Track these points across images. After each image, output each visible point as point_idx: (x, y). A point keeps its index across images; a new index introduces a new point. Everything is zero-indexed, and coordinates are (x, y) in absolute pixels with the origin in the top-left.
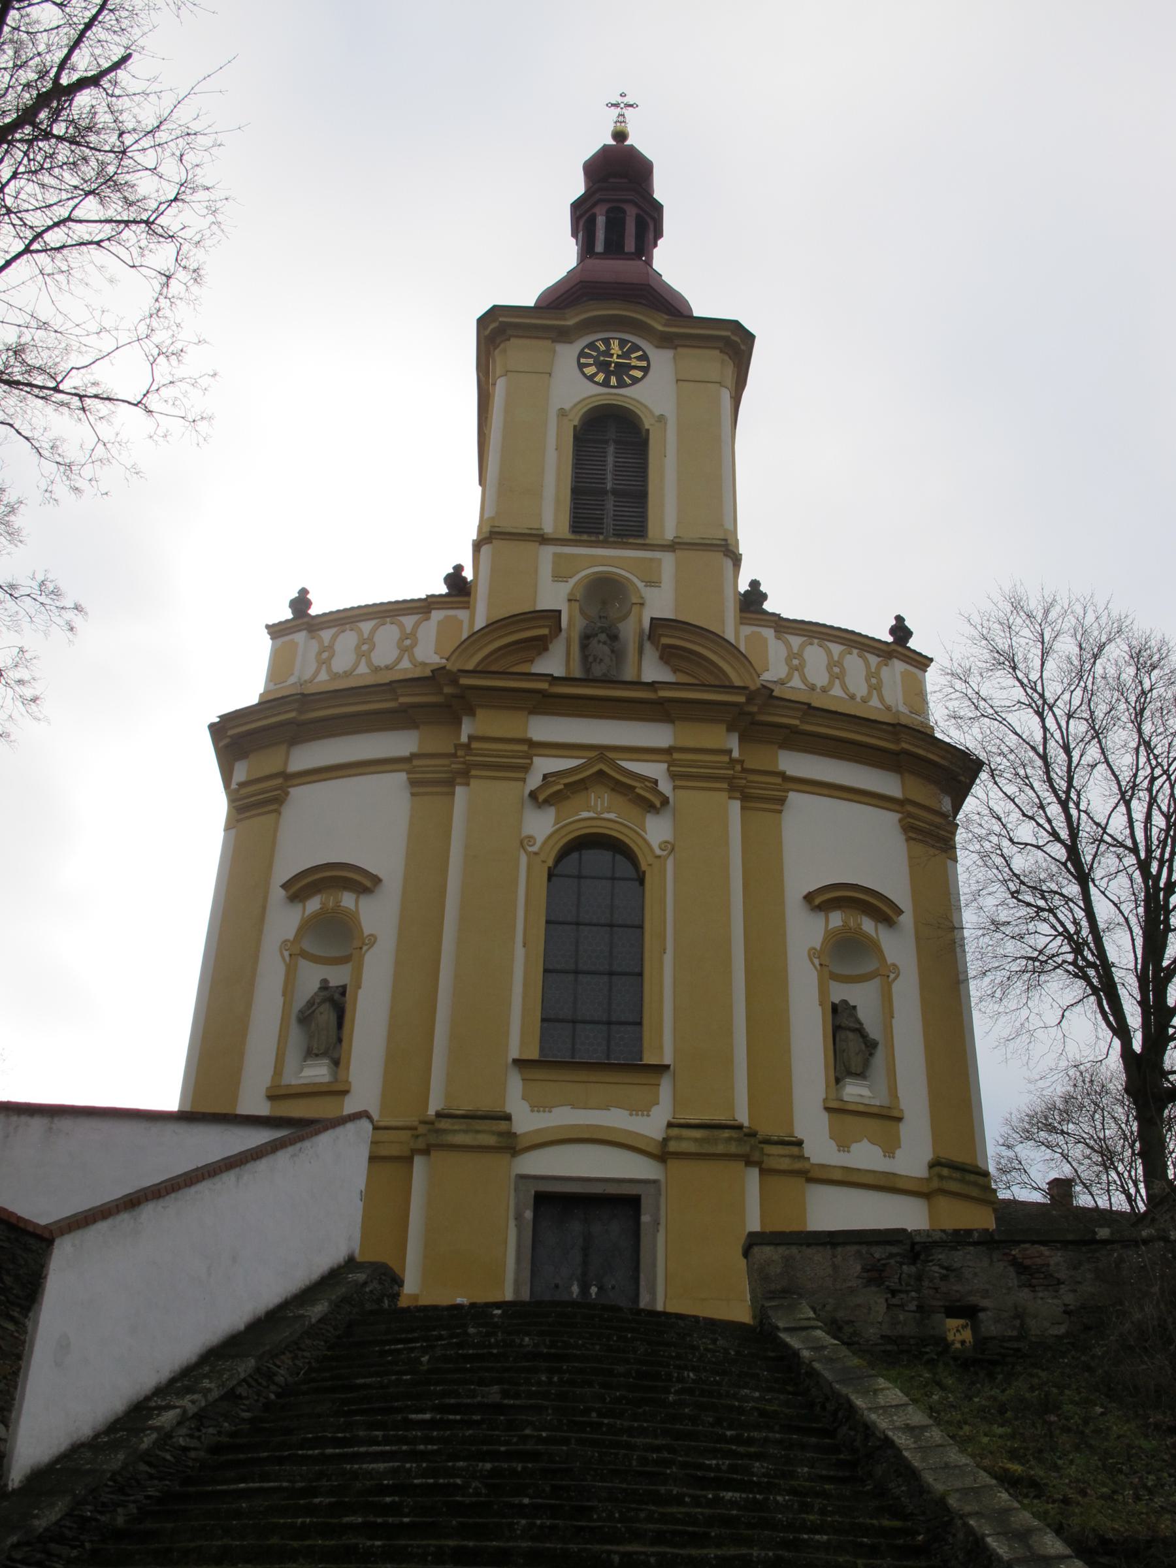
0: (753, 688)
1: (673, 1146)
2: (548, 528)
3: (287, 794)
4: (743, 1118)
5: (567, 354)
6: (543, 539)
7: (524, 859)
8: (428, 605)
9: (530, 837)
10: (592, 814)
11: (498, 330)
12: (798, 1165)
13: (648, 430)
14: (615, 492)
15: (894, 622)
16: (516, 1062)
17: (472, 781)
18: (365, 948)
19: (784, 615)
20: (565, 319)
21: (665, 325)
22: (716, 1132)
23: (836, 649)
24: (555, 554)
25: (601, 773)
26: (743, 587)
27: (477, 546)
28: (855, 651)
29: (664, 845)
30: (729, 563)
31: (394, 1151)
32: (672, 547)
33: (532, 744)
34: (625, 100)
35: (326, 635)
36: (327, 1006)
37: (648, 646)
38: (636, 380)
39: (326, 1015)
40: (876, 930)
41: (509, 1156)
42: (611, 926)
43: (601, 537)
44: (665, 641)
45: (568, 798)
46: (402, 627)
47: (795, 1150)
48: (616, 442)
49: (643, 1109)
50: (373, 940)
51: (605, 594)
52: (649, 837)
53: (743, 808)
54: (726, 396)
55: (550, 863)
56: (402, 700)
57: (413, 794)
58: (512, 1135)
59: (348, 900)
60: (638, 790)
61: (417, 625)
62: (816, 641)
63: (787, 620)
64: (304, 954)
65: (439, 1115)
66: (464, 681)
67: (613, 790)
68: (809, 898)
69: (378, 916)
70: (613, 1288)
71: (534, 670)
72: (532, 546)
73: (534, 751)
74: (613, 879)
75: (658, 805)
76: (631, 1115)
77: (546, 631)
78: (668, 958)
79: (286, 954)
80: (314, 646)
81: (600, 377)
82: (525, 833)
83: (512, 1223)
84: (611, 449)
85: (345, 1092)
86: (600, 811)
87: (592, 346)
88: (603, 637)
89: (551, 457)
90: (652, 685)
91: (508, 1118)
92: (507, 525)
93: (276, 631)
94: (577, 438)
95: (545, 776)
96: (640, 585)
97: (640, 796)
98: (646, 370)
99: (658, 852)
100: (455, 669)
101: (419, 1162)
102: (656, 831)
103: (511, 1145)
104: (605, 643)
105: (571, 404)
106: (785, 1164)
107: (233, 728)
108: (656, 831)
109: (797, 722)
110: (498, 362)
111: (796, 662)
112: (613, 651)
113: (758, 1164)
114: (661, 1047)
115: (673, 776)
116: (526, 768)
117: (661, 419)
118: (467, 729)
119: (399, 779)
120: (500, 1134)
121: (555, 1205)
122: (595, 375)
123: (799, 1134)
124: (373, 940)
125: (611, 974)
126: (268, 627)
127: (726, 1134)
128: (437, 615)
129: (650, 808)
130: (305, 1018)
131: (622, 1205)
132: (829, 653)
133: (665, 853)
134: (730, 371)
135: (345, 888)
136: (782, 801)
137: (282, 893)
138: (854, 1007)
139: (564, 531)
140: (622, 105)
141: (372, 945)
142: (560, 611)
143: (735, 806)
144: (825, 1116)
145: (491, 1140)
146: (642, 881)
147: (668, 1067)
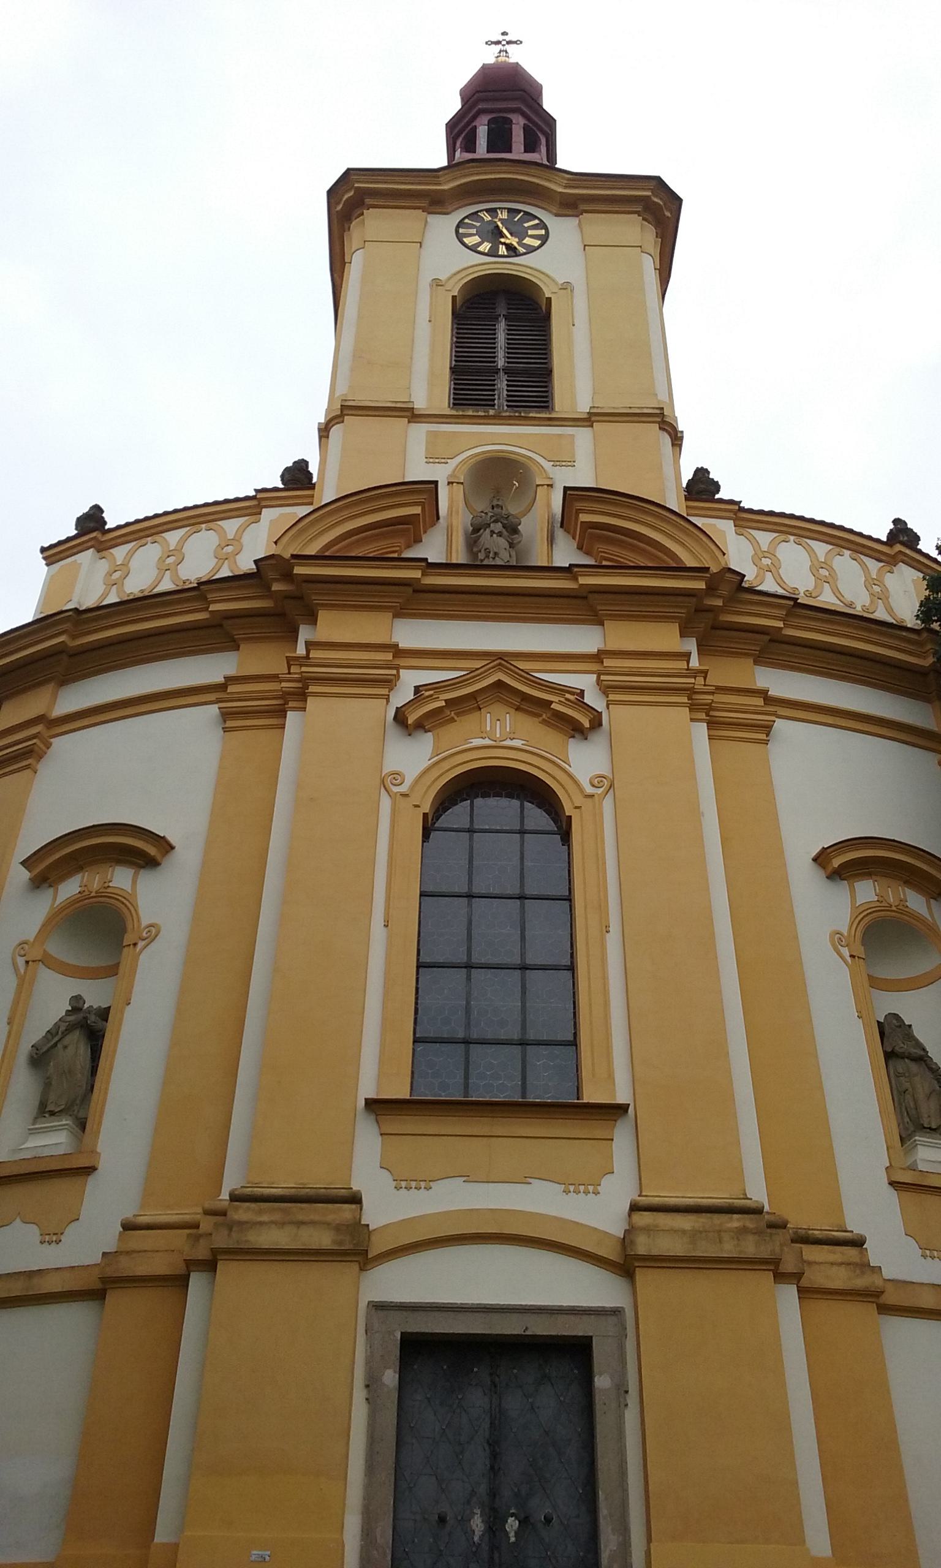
0: (714, 569)
1: (643, 1246)
2: (420, 403)
3: (48, 746)
4: (758, 1193)
5: (442, 226)
6: (412, 415)
7: (386, 803)
8: (254, 505)
10: (487, 742)
11: (356, 198)
12: (860, 1283)
13: (549, 300)
14: (507, 371)
15: (892, 526)
16: (374, 1105)
17: (309, 699)
18: (141, 944)
19: (745, 505)
20: (439, 184)
21: (566, 187)
22: (718, 1219)
23: (821, 549)
25: (499, 684)
26: (687, 475)
27: (324, 432)
28: (847, 553)
29: (597, 780)
30: (667, 440)
31: (159, 1266)
32: (589, 420)
33: (398, 652)
34: (508, 38)
35: (119, 553)
36: (76, 1035)
37: (560, 534)
38: (531, 250)
39: (77, 1048)
40: (929, 908)
41: (355, 1267)
43: (492, 412)
44: (584, 518)
45: (452, 720)
46: (222, 532)
47: (851, 1253)
48: (506, 318)
49: (586, 1183)
50: (153, 933)
51: (499, 476)
53: (711, 738)
55: (426, 807)
56: (212, 608)
57: (226, 730)
58: (358, 1229)
59: (121, 878)
61: (242, 529)
62: (792, 538)
63: (751, 511)
64: (47, 961)
65: (235, 1198)
66: (297, 570)
67: (518, 709)
68: (821, 858)
69: (161, 901)
70: (548, 1520)
71: (403, 556)
72: (399, 424)
73: (402, 662)
74: (522, 832)
75: (587, 725)
76: (567, 1192)
77: (417, 510)
78: (613, 940)
79: (21, 961)
80: (103, 566)
81: (486, 247)
83: (359, 1395)
84: (502, 326)
85: (90, 1170)
86: (500, 737)
87: (474, 215)
88: (498, 527)
89: (423, 331)
90: (569, 571)
91: (355, 1199)
92: (364, 398)
93: (53, 554)
94: (455, 314)
95: (417, 689)
96: (547, 465)
98: (544, 239)
99: (589, 790)
100: (287, 555)
101: (197, 1281)
102: (583, 763)
103: (357, 1250)
104: (500, 534)
105: (448, 275)
106: (840, 1279)
108: (583, 763)
109: (781, 624)
110: (356, 234)
111: (766, 562)
112: (511, 545)
113: (796, 1277)
114: (611, 1076)
115: (605, 689)
116: (390, 683)
117: (567, 287)
118: (305, 633)
120: (338, 1228)
121: (439, 1356)
122: (479, 244)
123: (855, 1225)
124: (153, 933)
125: (524, 968)
126: (43, 550)
127: (735, 1222)
128: (268, 514)
129: (576, 731)
130: (39, 1058)
131: (559, 1354)
132: (811, 552)
134: (649, 236)
135: (119, 862)
136: (767, 728)
137: (25, 875)
138: (910, 1026)
139: (442, 402)
140: (504, 42)
141: (151, 939)
142: (436, 483)
143: (701, 730)
144: (892, 1195)
145: (324, 1239)
146: (566, 836)
147: (622, 1109)
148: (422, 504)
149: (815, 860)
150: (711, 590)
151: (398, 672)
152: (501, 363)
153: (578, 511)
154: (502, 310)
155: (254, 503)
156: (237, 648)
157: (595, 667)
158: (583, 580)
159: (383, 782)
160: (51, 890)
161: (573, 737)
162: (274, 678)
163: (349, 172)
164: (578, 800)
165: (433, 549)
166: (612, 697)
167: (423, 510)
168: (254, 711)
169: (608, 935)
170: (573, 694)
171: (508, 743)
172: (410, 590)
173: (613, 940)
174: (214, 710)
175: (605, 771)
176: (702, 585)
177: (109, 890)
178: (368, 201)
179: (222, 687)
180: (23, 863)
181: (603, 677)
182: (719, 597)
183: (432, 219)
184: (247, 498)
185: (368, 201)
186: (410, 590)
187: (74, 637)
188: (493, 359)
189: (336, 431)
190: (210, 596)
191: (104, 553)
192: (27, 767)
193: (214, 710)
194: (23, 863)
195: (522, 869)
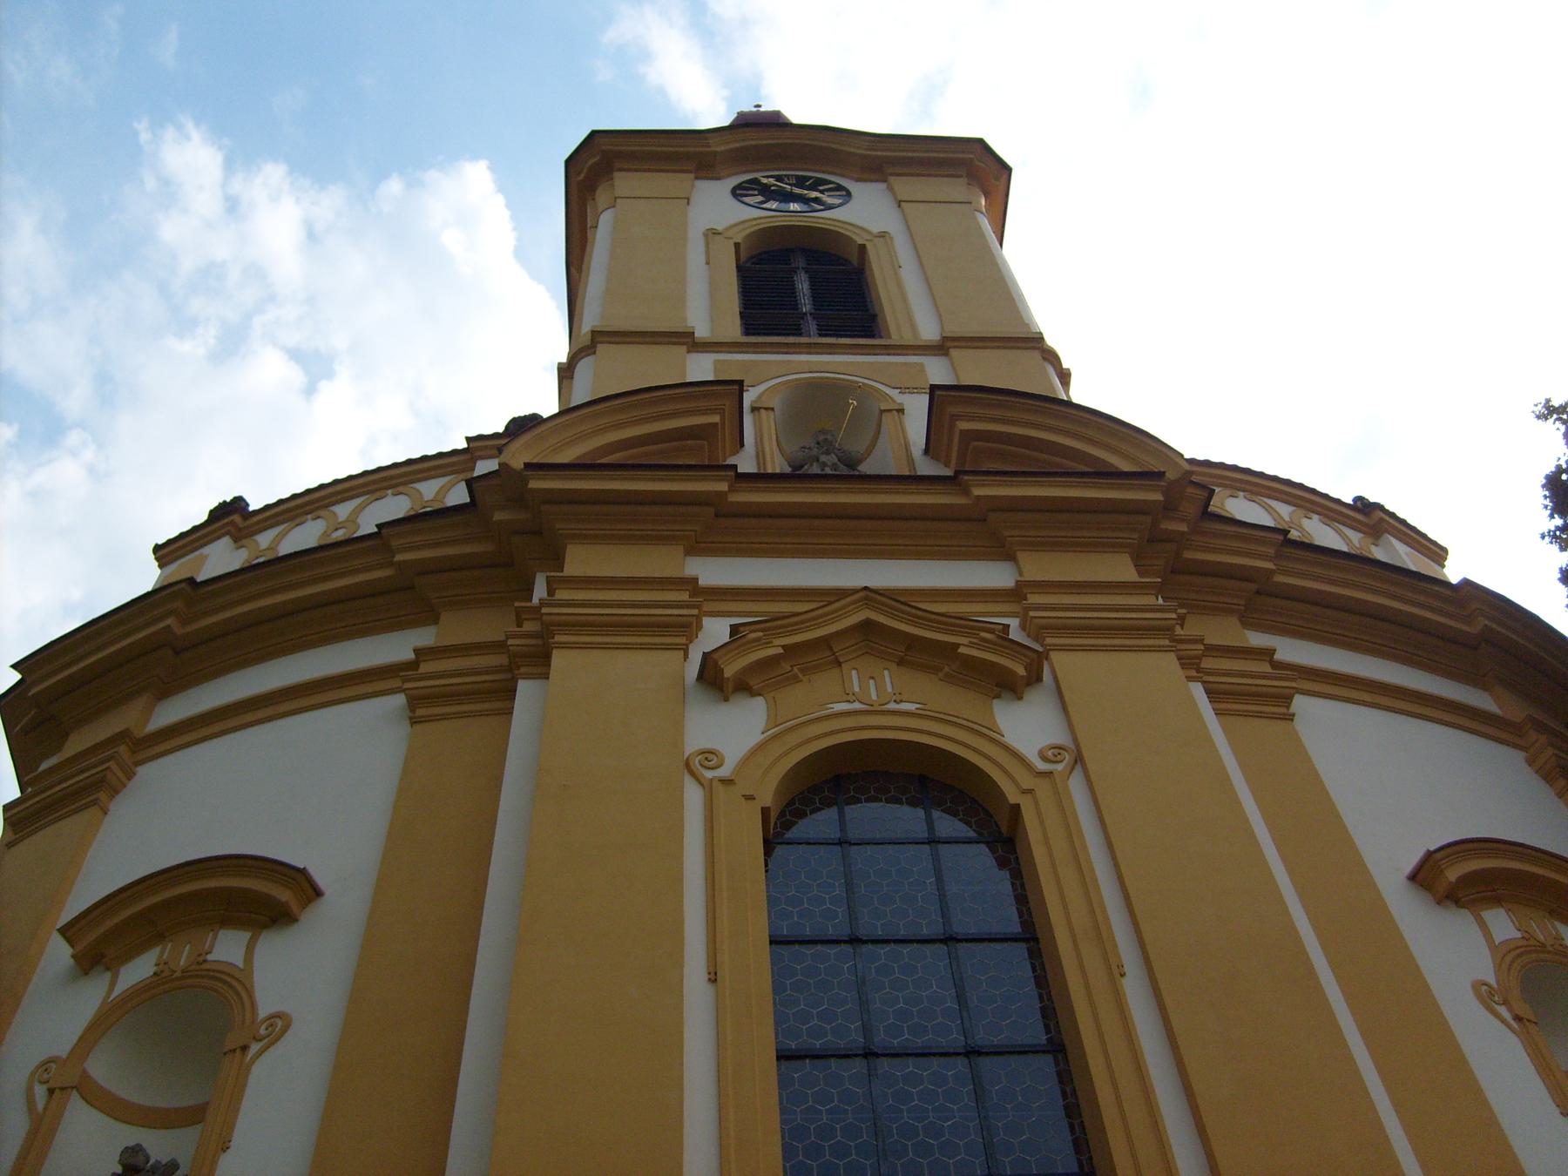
0: (1171, 475)
2: (702, 332)
3: (130, 775)
7: (693, 796)
9: (708, 753)
10: (857, 706)
13: (862, 248)
18: (255, 1048)
24: (716, 362)
25: (867, 625)
29: (1052, 753)
42: (949, 939)
44: (964, 425)
52: (1011, 739)
54: (985, 224)
55: (767, 797)
56: (399, 558)
57: (414, 721)
59: (228, 947)
60: (962, 650)
67: (901, 663)
69: (299, 978)
73: (707, 607)
75: (1021, 671)
77: (716, 419)
78: (1134, 988)
79: (40, 1092)
82: (694, 741)
86: (875, 701)
95: (734, 630)
96: (894, 393)
97: (969, 662)
99: (1041, 766)
102: (1026, 727)
107: (39, 681)
109: (1269, 565)
110: (602, 196)
115: (1038, 632)
116: (688, 629)
117: (882, 235)
119: (382, 713)
124: (280, 1024)
126: (157, 549)
133: (1060, 767)
135: (226, 923)
139: (732, 328)
141: (273, 1038)
143: (1198, 690)
148: (722, 412)
149: (1413, 877)
150: (1169, 508)
151: (698, 618)
152: (806, 305)
153: (954, 418)
154: (801, 263)
155: (467, 456)
156: (436, 621)
157: (1015, 608)
158: (977, 492)
159: (687, 765)
160: (108, 975)
161: (998, 696)
162: (499, 646)
163: (594, 134)
164: (1027, 782)
165: (746, 463)
166: (1049, 641)
167: (723, 419)
168: (462, 699)
169: (1124, 981)
170: (991, 631)
171: (892, 706)
172: (711, 510)
173: (1134, 988)
174: (400, 699)
175: (1062, 738)
176: (1158, 497)
177: (204, 966)
178: (617, 165)
179: (412, 665)
180: (63, 931)
181: (1032, 614)
182: (1182, 520)
183: (699, 183)
184: (455, 452)
185: (617, 165)
186: (711, 510)
187: (184, 623)
188: (795, 305)
189: (584, 368)
190: (395, 543)
191: (245, 542)
192: (95, 802)
193: (400, 699)
194: (63, 931)
195: (942, 897)
